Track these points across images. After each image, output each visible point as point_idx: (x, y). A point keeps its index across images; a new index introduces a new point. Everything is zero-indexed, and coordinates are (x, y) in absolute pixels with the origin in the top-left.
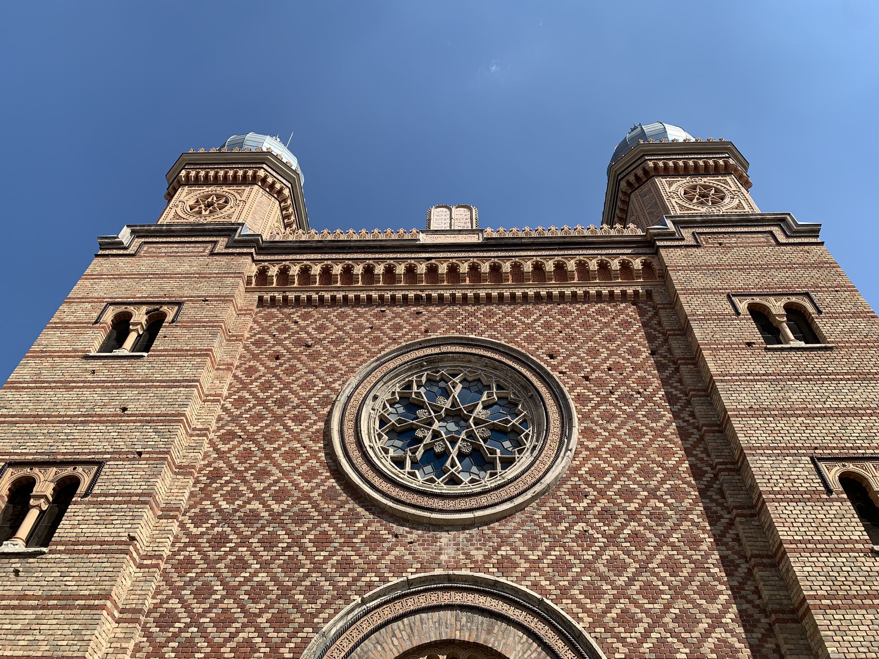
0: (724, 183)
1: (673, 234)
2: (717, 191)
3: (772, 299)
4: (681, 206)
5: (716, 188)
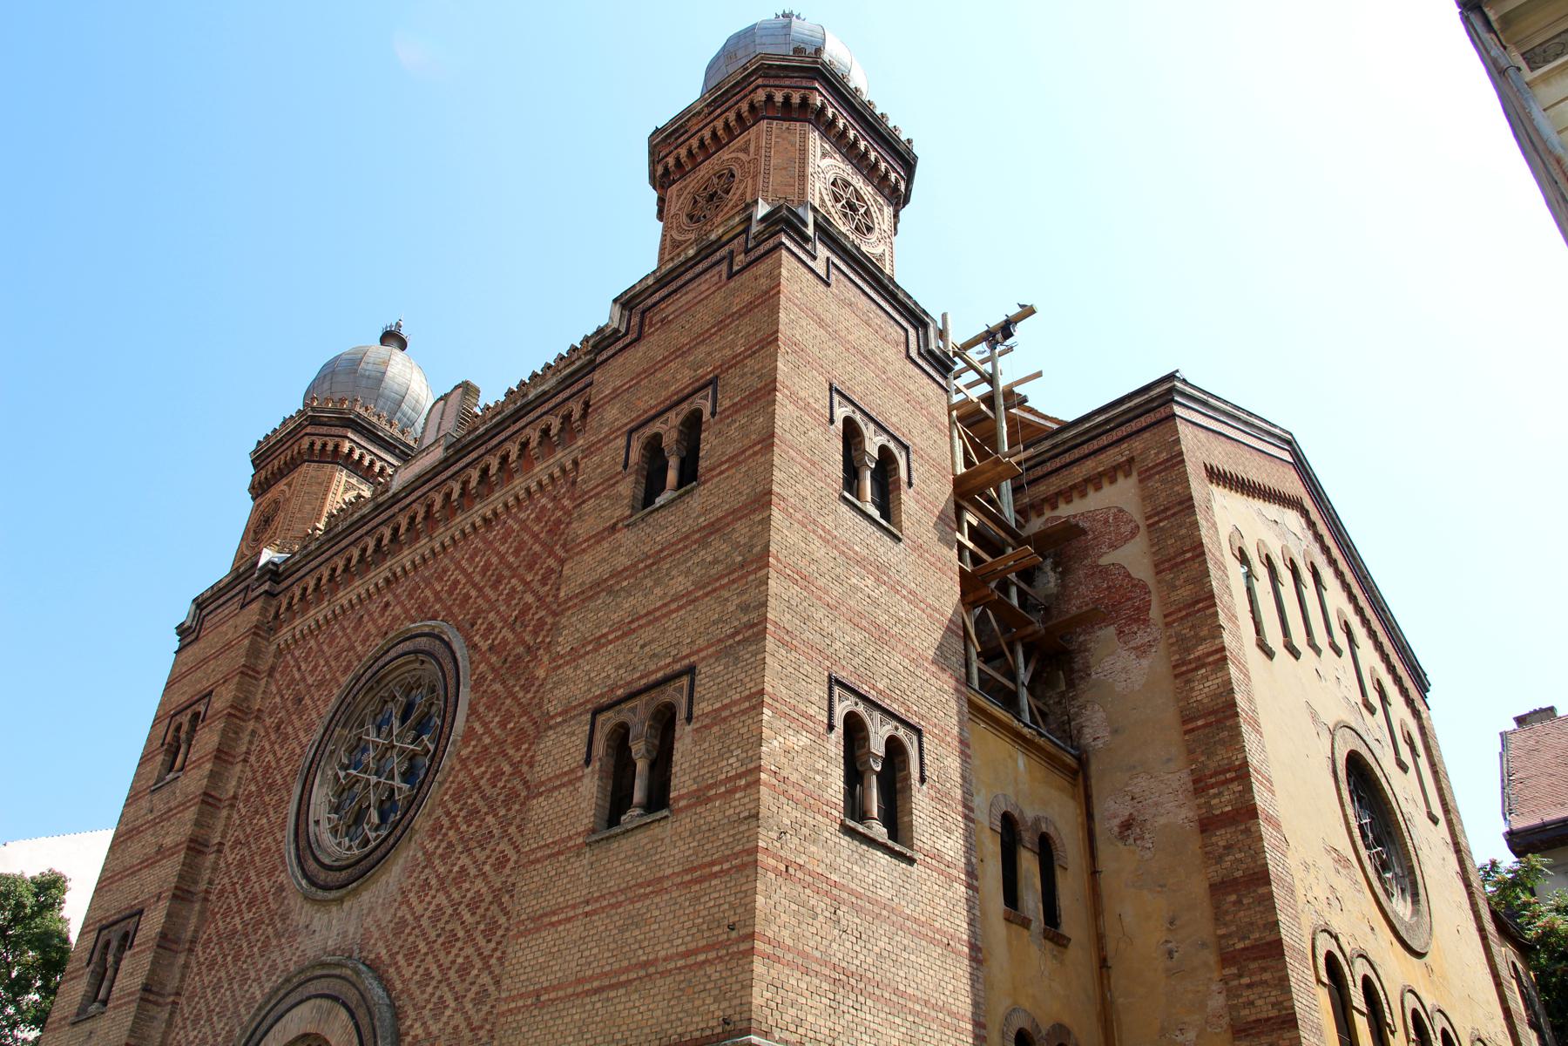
0: (879, 210)
1: (807, 239)
2: (867, 212)
3: (872, 426)
4: (822, 200)
5: (868, 208)
